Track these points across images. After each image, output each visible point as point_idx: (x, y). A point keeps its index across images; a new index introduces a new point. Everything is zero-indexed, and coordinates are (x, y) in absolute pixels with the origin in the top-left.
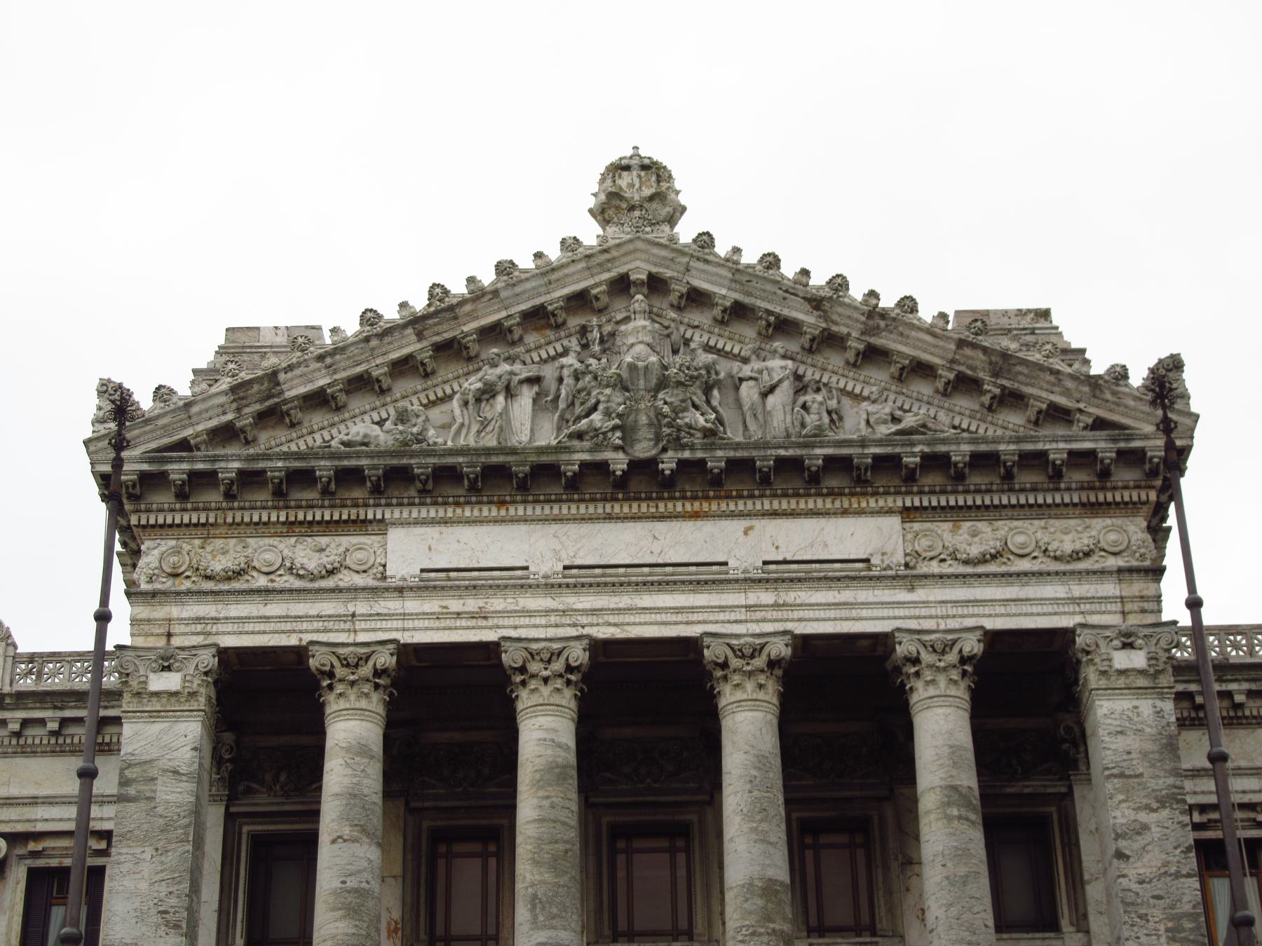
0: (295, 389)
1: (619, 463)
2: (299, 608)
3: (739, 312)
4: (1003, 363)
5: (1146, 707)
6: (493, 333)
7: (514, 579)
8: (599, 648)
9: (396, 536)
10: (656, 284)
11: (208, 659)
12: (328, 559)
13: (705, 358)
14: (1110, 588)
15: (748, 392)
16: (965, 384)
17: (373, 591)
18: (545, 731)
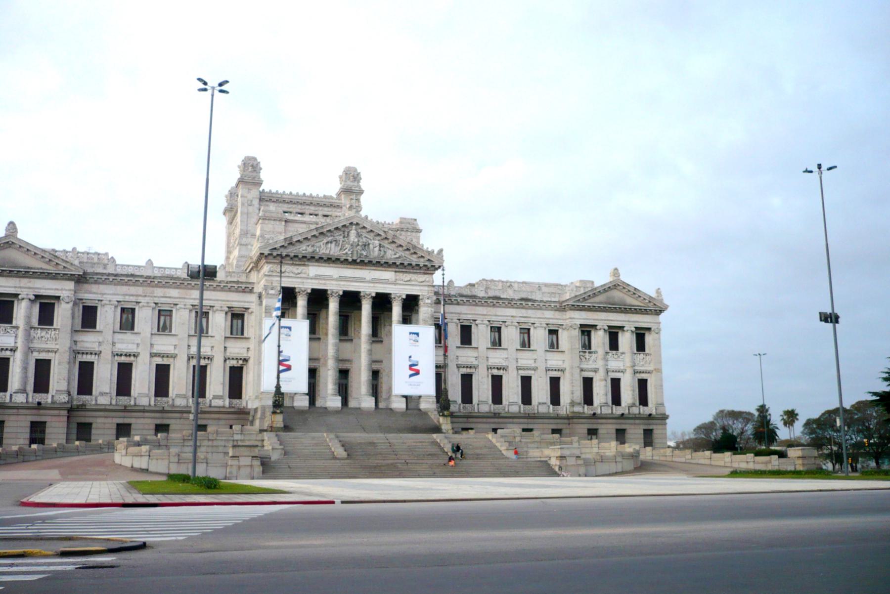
0: (295, 239)
1: (350, 259)
2: (294, 280)
3: (371, 231)
4: (415, 247)
5: (430, 309)
6: (329, 231)
7: (330, 278)
8: (345, 292)
9: (310, 268)
10: (357, 224)
11: (279, 288)
12: (299, 271)
13: (364, 240)
14: (426, 288)
15: (371, 246)
16: (408, 250)
17: (308, 278)
18: (333, 305)
